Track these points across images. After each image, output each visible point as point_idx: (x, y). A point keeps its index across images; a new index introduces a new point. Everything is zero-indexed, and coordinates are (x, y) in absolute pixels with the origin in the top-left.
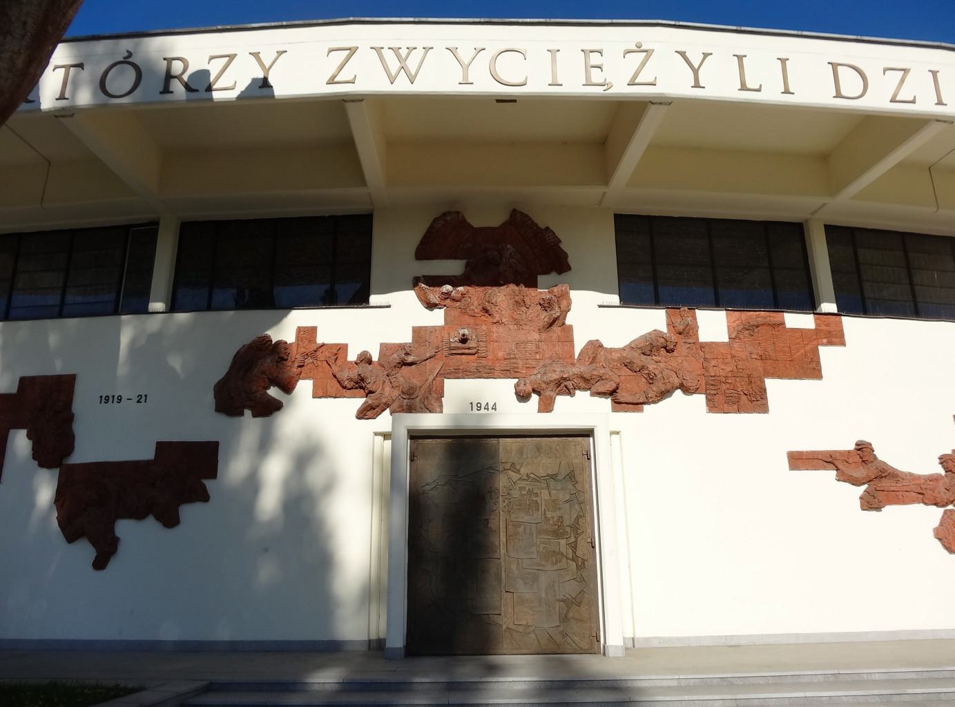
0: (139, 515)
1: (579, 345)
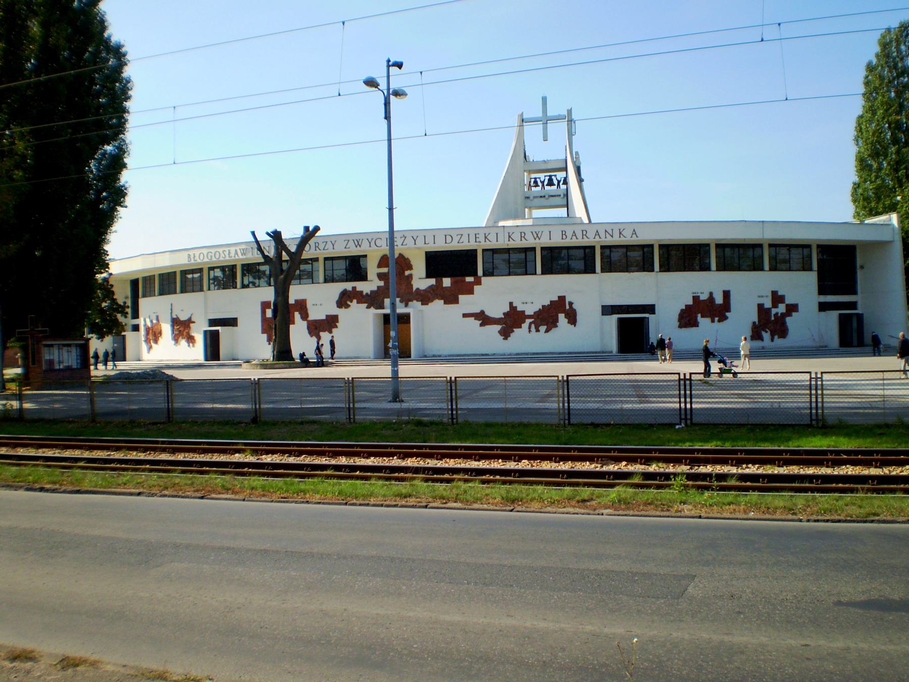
0: (324, 331)
1: (414, 289)
